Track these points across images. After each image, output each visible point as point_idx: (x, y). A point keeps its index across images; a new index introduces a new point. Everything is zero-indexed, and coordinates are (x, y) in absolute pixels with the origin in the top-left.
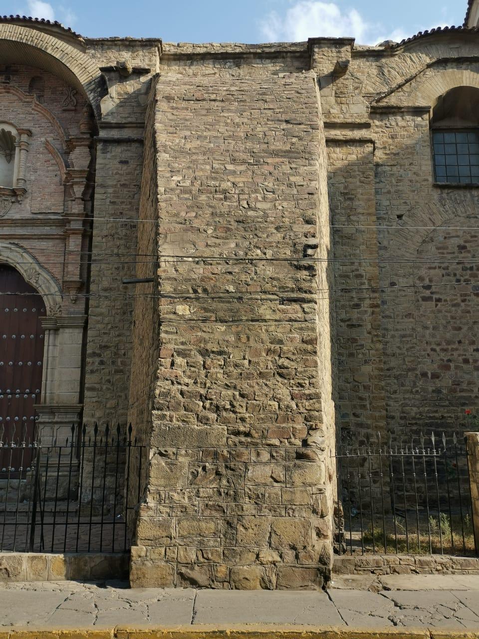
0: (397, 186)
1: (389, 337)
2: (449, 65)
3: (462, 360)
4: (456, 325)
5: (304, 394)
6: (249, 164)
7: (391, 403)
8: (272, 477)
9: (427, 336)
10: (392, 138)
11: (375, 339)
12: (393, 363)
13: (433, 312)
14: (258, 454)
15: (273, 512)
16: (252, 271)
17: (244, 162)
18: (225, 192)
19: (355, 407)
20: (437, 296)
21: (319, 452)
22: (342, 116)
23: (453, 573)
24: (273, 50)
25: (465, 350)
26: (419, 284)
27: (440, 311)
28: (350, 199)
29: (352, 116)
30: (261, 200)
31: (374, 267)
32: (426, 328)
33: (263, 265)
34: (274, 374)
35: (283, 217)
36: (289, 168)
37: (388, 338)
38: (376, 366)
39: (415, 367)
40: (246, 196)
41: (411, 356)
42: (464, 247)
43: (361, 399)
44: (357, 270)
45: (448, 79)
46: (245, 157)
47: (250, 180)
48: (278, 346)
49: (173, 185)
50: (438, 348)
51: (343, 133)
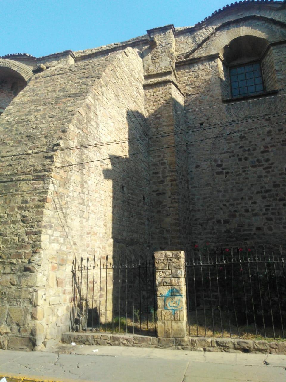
0: (200, 106)
2: (231, 26)
3: (244, 211)
5: (33, 232)
6: (52, 104)
7: (198, 241)
8: (10, 282)
11: (173, 201)
14: (4, 269)
15: (9, 303)
18: (28, 121)
20: (226, 171)
21: (36, 267)
22: (156, 70)
23: (133, 346)
25: (246, 204)
27: (228, 180)
31: (172, 157)
35: (51, 130)
38: (173, 217)
41: (210, 210)
43: (165, 238)
44: (162, 160)
45: (230, 34)
48: (24, 205)
49: (4, 121)
50: (227, 204)
51: (156, 80)
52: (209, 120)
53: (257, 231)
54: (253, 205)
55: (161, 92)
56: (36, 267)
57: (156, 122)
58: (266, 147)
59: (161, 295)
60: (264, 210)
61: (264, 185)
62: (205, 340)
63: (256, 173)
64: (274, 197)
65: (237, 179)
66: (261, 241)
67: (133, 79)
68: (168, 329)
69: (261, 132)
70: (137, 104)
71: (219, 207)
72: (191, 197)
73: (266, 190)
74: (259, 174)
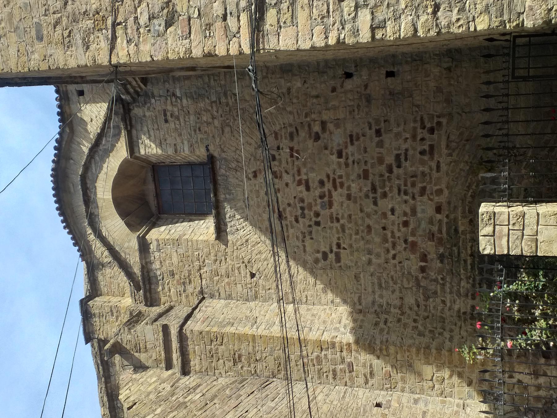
4: (366, 231)
9: (379, 261)
10: (173, 275)
12: (410, 300)
13: (352, 253)
26: (322, 263)
27: (351, 246)
29: (157, 340)
32: (370, 262)
39: (414, 278)
41: (402, 281)
44: (312, 360)
50: (392, 252)
51: (174, 351)
53: (442, 212)
54: (396, 213)
55: (197, 347)
58: (299, 183)
60: (405, 197)
61: (363, 193)
63: (342, 202)
64: (384, 181)
65: (351, 231)
66: (460, 209)
67: (174, 398)
70: (216, 396)
71: (397, 266)
72: (376, 307)
73: (372, 190)
74: (344, 199)
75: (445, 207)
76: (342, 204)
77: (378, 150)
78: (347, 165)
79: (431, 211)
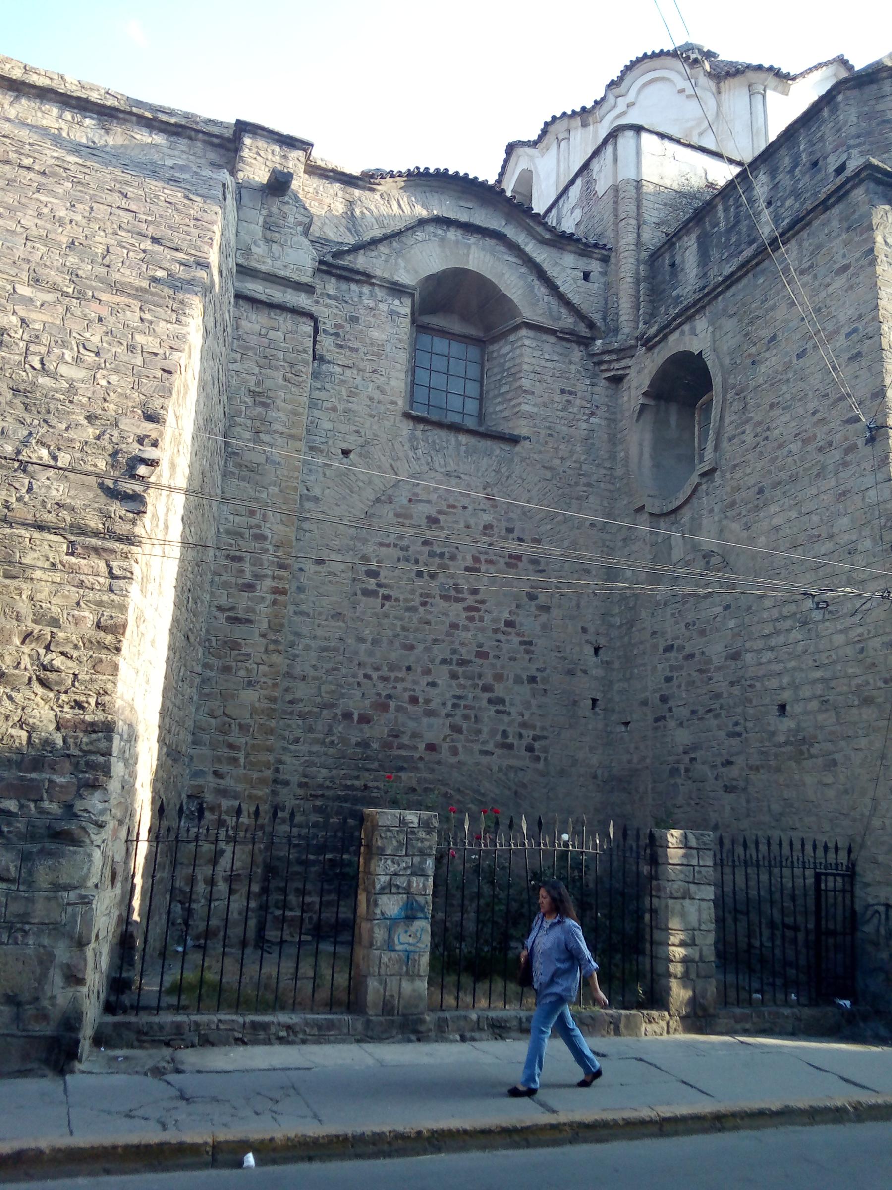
0: (348, 401)
1: (301, 647)
3: (407, 698)
5: (83, 721)
7: (287, 758)
12: (302, 691)
13: (376, 616)
16: (23, 485)
17: (55, 288)
19: (219, 759)
21: (92, 829)
23: (304, 1042)
24: (173, 120)
25: (415, 682)
27: (386, 616)
28: (264, 404)
30: (70, 361)
32: (361, 640)
33: (48, 479)
34: (30, 679)
35: (105, 400)
36: (137, 319)
37: (299, 650)
40: (43, 349)
41: (331, 683)
42: (436, 521)
43: (231, 746)
46: (59, 280)
47: (58, 322)
48: (47, 630)
50: (375, 675)
52: (366, 448)
54: (429, 689)
56: (92, 829)
57: (255, 412)
58: (476, 559)
59: (382, 914)
60: (449, 704)
62: (466, 1018)
64: (473, 678)
66: (430, 776)
68: (392, 996)
69: (472, 522)
74: (452, 618)
75: (434, 756)
76: (446, 614)
77: (512, 676)
78: (496, 631)
79: (430, 737)
